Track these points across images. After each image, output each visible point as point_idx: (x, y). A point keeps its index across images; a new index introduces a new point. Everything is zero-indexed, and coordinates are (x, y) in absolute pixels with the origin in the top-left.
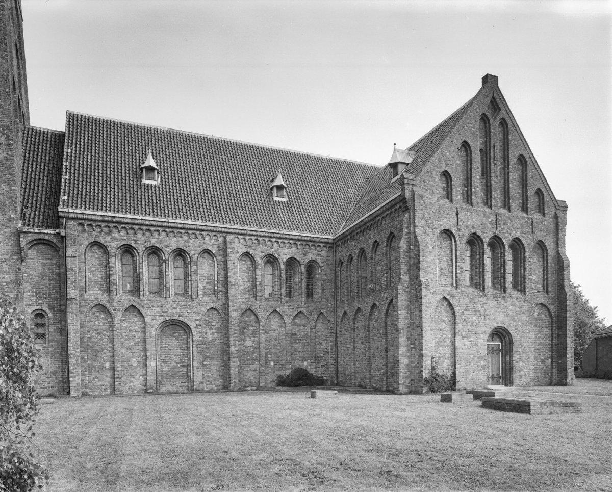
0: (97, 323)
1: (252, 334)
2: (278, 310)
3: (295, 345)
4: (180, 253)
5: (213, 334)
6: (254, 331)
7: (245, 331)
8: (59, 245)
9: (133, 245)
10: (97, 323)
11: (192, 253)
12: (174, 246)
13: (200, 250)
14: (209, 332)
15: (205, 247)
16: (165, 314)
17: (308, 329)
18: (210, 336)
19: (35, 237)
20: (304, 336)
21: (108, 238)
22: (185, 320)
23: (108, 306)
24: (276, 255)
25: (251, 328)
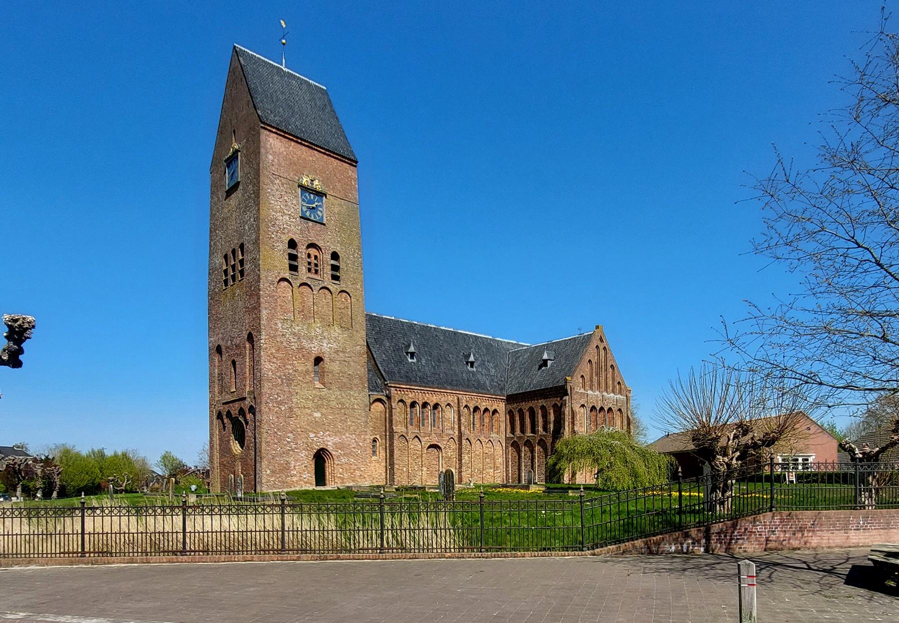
4: (436, 406)
12: (435, 402)
13: (446, 404)
15: (448, 402)
22: (439, 444)
23: (406, 436)
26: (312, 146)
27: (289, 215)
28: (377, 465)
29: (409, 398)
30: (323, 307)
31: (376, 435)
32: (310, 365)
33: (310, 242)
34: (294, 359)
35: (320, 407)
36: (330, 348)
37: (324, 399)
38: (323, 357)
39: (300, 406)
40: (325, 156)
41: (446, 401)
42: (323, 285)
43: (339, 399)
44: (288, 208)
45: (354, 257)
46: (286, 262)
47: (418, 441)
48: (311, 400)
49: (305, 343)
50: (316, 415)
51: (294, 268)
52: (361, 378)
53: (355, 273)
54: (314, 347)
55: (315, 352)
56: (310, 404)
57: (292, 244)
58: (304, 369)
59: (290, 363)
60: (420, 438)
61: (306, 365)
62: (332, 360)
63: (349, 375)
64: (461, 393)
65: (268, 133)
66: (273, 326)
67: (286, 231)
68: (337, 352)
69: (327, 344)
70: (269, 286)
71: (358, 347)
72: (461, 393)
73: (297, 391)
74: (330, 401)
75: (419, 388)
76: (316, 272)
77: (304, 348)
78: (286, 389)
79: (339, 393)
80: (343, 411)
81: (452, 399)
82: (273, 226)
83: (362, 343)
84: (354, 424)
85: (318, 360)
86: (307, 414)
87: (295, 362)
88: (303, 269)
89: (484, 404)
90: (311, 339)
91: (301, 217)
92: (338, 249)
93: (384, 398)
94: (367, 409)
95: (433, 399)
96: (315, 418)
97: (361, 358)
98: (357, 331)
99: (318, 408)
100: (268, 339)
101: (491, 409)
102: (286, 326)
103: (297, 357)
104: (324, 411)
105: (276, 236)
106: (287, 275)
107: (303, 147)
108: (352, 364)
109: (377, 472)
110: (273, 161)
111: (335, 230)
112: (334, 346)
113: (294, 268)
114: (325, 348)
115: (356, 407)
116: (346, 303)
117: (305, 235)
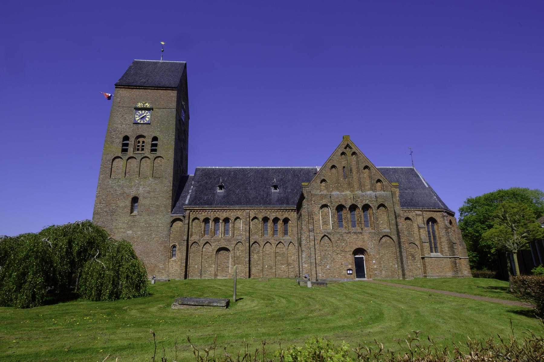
0: (194, 249)
1: (257, 253)
2: (269, 241)
3: (278, 258)
4: (227, 220)
5: (240, 253)
6: (258, 251)
7: (254, 251)
8: (183, 220)
9: (209, 218)
10: (194, 249)
11: (232, 219)
12: (225, 217)
13: (235, 217)
14: (238, 252)
16: (220, 245)
17: (284, 249)
18: (238, 254)
19: (175, 217)
20: (282, 253)
21: (200, 216)
22: (227, 247)
23: (198, 242)
24: (268, 217)
25: (257, 250)
26: (145, 87)
27: (126, 124)
28: (174, 264)
29: (202, 216)
30: (144, 168)
31: (175, 242)
32: (128, 203)
33: (138, 135)
34: (117, 200)
35: (132, 227)
36: (144, 191)
37: (136, 222)
38: (138, 197)
39: (117, 227)
40: (155, 90)
41: (235, 216)
42: (144, 156)
43: (147, 221)
44: (125, 121)
45: (169, 136)
46: (120, 147)
47: (209, 245)
48: (126, 223)
49: (126, 190)
50: (128, 232)
51: (124, 150)
52: (165, 206)
53: (169, 145)
54: (133, 191)
55: (133, 193)
56: (125, 226)
57: (126, 138)
58: (124, 205)
59: (114, 202)
60: (211, 243)
61: (126, 203)
62: (145, 198)
63: (157, 205)
64: (249, 208)
65: (119, 89)
66: (106, 183)
67: (123, 132)
68: (149, 192)
69: (142, 189)
70: (107, 162)
71: (165, 188)
72: (249, 208)
73: (117, 218)
74: (140, 223)
75: (210, 208)
76: (143, 150)
77: (125, 193)
78: (109, 218)
79: (147, 217)
80: (149, 229)
81: (239, 214)
82: (115, 131)
83: (169, 184)
84: (157, 236)
85: (135, 200)
86: (122, 232)
87: (118, 202)
88: (131, 149)
89: (274, 214)
90: (131, 187)
91: (134, 123)
92: (157, 134)
93: (182, 218)
94: (169, 226)
95: (223, 215)
96: (127, 234)
97: (167, 194)
98: (166, 178)
99: (130, 228)
100: (101, 190)
101: (282, 218)
102: (114, 182)
103: (120, 198)
104: (135, 229)
105: (116, 136)
106: (120, 154)
107: (141, 90)
108: (160, 198)
109: (174, 269)
110: (120, 101)
111: (157, 125)
112: (148, 189)
113: (124, 150)
114: (141, 191)
115: (160, 225)
116: (160, 163)
117: (135, 132)
